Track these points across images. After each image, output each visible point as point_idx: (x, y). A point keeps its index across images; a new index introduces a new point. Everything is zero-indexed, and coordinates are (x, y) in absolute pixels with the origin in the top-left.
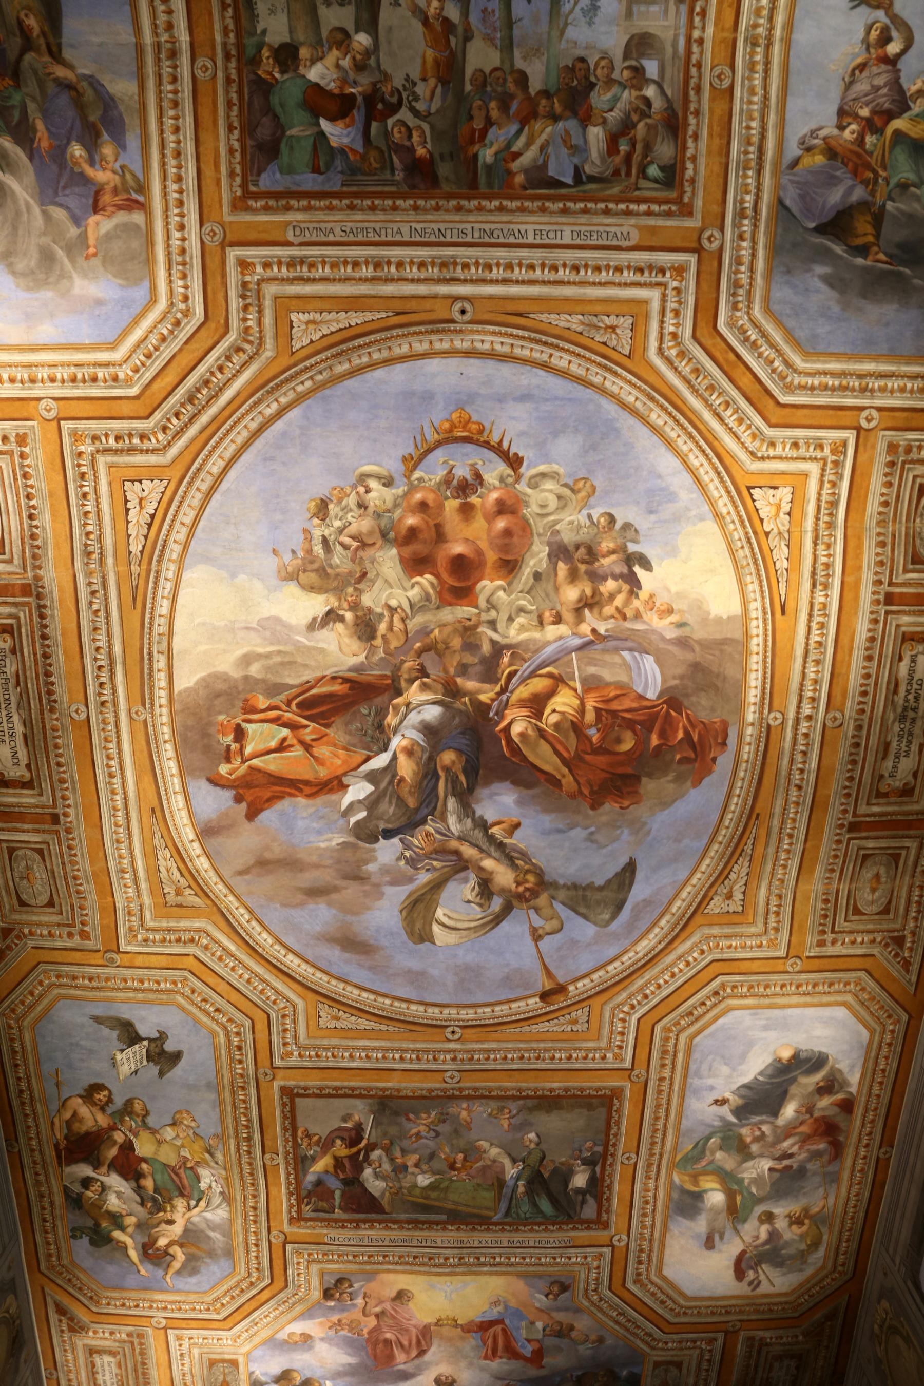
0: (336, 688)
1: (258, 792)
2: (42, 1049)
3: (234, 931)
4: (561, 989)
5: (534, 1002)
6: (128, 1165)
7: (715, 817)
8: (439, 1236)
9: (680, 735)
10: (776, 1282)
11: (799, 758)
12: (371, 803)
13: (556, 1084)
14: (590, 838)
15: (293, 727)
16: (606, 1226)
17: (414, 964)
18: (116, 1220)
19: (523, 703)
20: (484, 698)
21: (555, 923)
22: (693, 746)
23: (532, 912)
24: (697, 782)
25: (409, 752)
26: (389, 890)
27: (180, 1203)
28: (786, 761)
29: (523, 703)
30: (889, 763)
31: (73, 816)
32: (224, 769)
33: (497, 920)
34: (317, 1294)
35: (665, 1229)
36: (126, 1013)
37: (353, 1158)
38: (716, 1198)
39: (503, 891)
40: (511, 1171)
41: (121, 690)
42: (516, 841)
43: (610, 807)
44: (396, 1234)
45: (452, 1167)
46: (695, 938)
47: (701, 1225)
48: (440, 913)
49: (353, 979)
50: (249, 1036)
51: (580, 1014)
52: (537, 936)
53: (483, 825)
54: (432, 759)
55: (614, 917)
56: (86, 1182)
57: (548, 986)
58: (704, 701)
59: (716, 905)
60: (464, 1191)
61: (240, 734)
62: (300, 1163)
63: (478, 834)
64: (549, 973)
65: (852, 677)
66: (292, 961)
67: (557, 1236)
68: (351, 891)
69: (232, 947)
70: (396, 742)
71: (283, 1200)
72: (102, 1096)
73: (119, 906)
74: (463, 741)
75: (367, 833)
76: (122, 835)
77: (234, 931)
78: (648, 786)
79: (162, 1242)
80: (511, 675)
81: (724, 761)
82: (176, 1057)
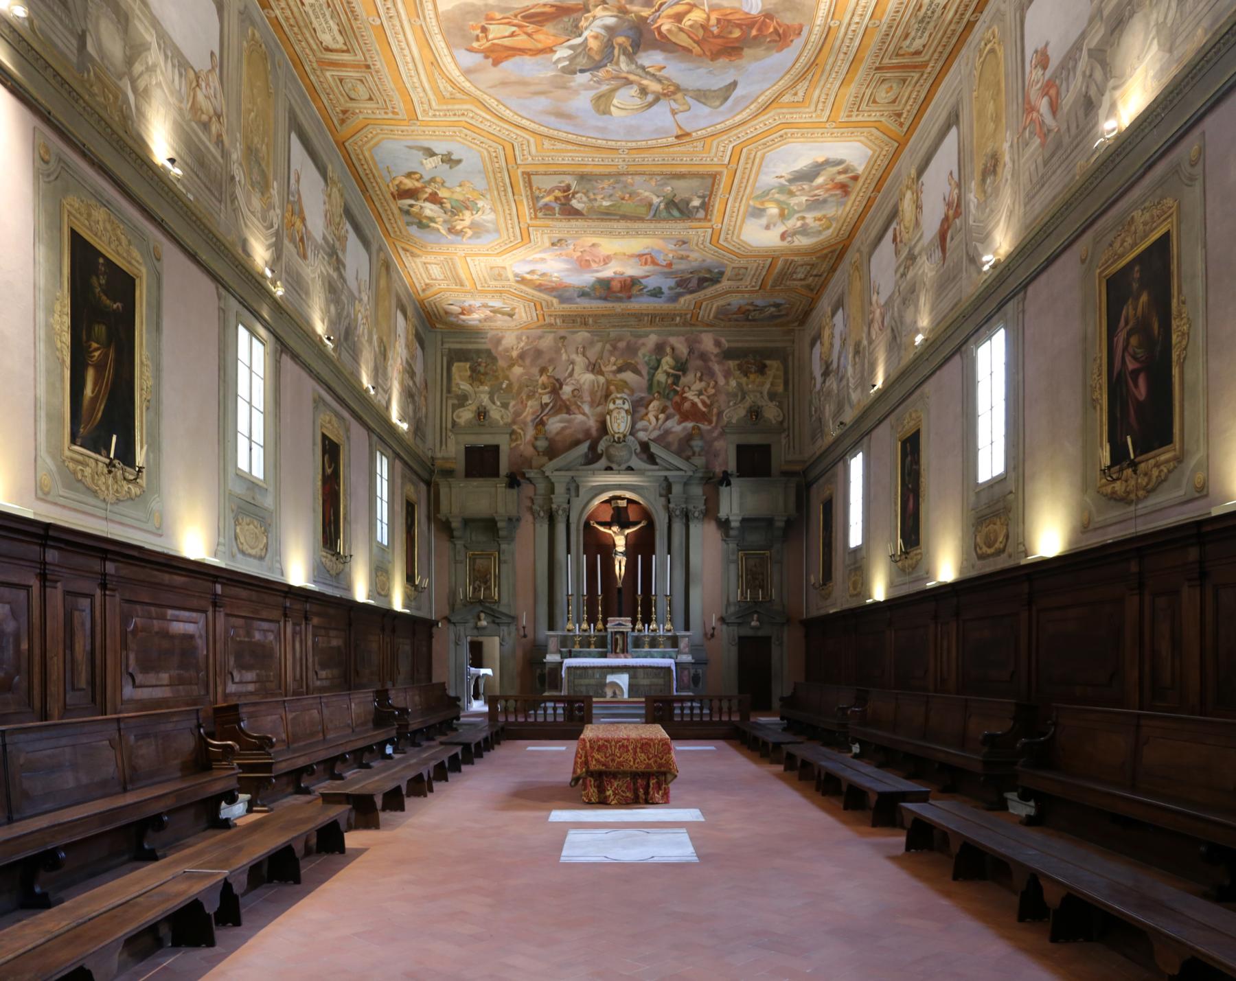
0: (547, 9)
1: (497, 54)
2: (377, 158)
3: (488, 109)
4: (688, 134)
5: (672, 140)
6: (434, 199)
7: (790, 64)
8: (615, 225)
9: (771, 30)
10: (802, 242)
11: (847, 42)
12: (572, 59)
13: (684, 170)
14: (710, 72)
15: (519, 26)
16: (710, 221)
17: (600, 124)
18: (432, 219)
19: (669, 17)
20: (643, 14)
21: (686, 107)
22: (779, 35)
23: (672, 102)
24: (780, 49)
25: (596, 37)
26: (583, 92)
27: (467, 213)
28: (838, 43)
29: (669, 17)
30: (908, 42)
31: (379, 63)
32: (475, 45)
33: (651, 105)
34: (547, 244)
35: (743, 222)
36: (426, 144)
37: (566, 197)
38: (773, 210)
39: (653, 92)
40: (656, 200)
41: (402, 11)
42: (663, 73)
43: (722, 61)
44: (591, 223)
45: (623, 199)
46: (772, 114)
47: (764, 221)
48: (615, 102)
49: (564, 129)
50: (502, 153)
51: (700, 144)
52: (674, 113)
53: (643, 68)
54: (610, 40)
55: (722, 104)
56: (411, 206)
57: (680, 133)
58: (789, 15)
59: (787, 98)
60: (628, 207)
61: (484, 30)
62: (535, 199)
63: (640, 71)
64: (680, 128)
65: (890, 5)
66: (525, 123)
67: (681, 225)
68: (559, 92)
69: (488, 117)
70: (586, 34)
71: (526, 210)
72: (417, 176)
73: (415, 100)
74: (630, 33)
75: (570, 71)
76: (413, 73)
77: (488, 109)
78: (746, 52)
79: (459, 228)
80: (661, 5)
81: (798, 43)
82: (459, 161)
